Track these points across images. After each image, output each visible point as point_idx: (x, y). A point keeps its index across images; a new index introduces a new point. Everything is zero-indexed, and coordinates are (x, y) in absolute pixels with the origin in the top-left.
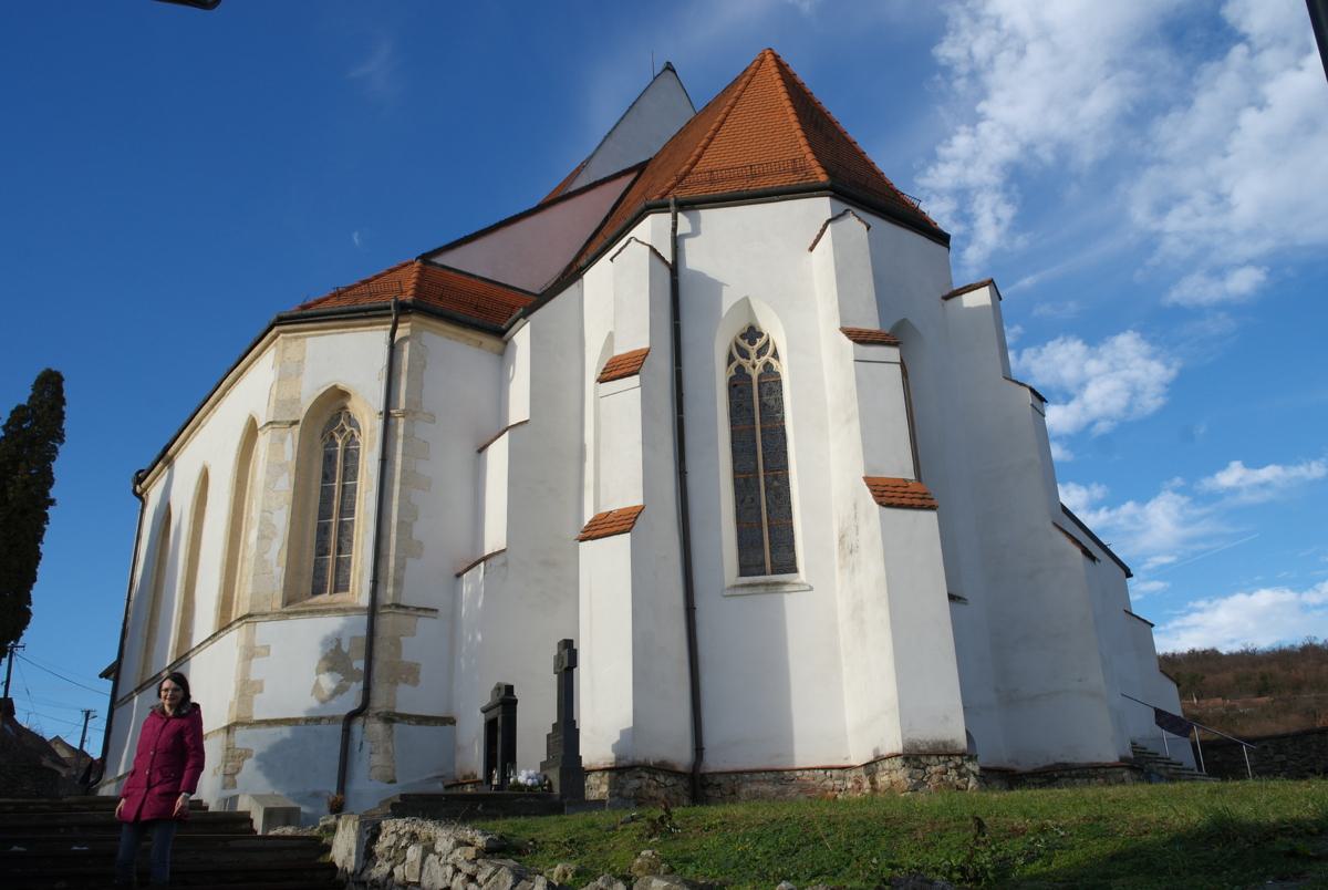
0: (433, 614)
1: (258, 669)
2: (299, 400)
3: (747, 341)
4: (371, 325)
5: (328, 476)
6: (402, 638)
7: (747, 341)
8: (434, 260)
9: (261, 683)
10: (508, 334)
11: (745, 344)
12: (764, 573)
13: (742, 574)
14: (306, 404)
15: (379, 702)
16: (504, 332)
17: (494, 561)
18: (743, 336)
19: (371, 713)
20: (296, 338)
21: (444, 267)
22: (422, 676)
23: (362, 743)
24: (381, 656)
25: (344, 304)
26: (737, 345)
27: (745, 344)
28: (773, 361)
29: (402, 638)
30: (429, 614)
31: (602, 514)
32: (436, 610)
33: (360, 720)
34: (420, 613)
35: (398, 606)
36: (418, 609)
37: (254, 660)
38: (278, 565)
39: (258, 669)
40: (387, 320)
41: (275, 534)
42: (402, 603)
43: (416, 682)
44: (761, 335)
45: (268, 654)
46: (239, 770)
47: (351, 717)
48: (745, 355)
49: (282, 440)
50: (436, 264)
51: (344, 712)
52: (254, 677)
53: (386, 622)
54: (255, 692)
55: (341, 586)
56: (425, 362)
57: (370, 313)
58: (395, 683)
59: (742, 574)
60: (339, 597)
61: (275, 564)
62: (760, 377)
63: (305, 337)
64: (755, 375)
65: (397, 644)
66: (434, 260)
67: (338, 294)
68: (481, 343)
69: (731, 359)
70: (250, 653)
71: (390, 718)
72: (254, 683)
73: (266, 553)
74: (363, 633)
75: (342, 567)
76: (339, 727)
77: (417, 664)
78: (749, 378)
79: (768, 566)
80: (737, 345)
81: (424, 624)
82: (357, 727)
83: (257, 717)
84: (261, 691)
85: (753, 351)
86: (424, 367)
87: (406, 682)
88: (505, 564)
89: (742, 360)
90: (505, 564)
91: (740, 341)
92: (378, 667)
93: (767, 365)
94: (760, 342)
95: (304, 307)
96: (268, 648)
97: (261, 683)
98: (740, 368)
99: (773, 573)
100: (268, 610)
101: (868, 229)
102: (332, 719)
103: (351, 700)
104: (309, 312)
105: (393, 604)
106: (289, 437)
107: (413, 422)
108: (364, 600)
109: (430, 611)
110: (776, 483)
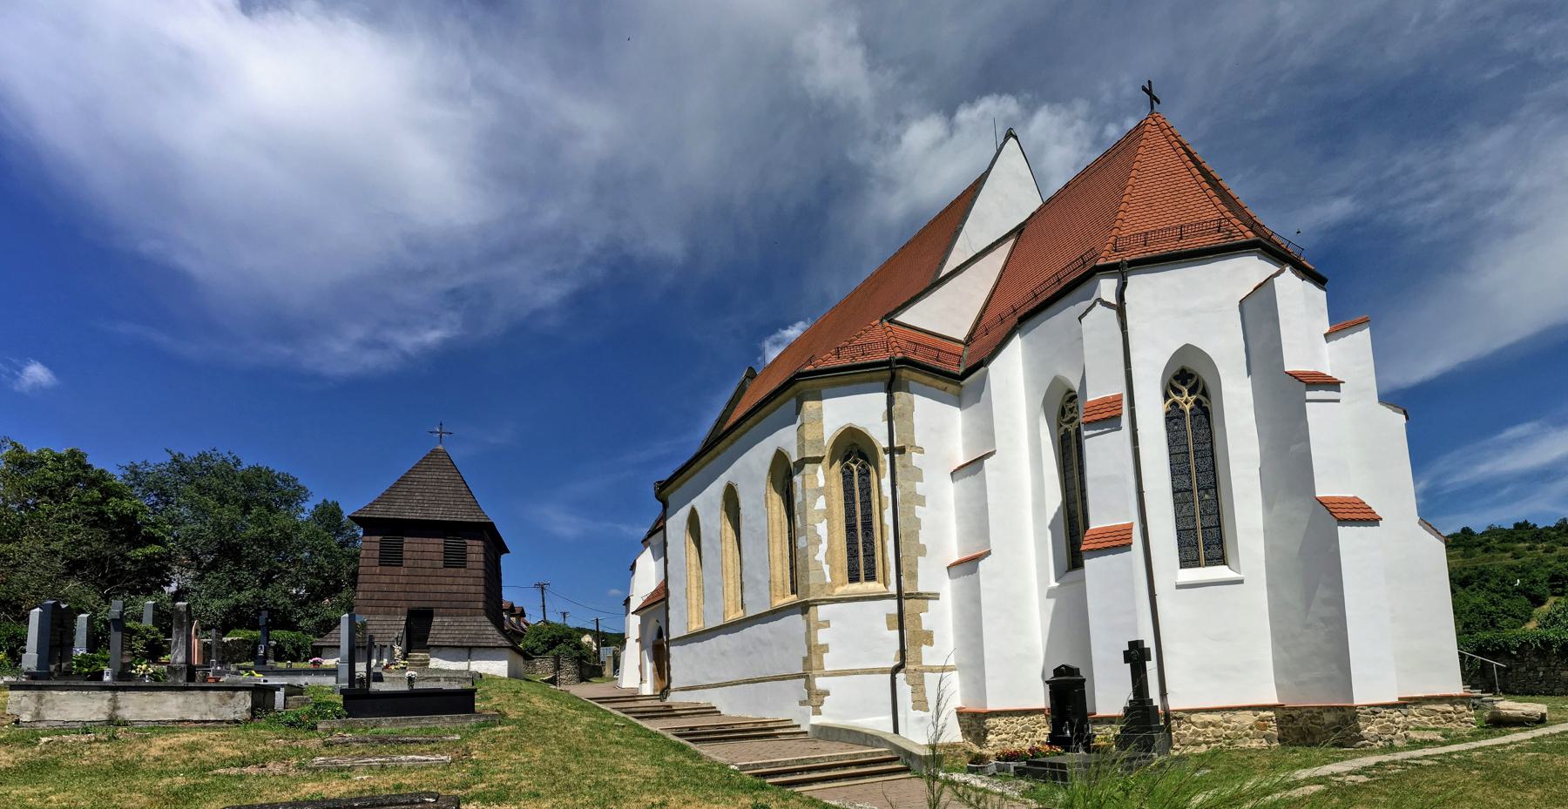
18: (1176, 378)
28: (1203, 398)
37: (819, 631)
39: (822, 636)
44: (1191, 376)
49: (816, 471)
53: (907, 604)
54: (824, 652)
59: (1186, 563)
61: (824, 562)
62: (1191, 410)
69: (1166, 397)
72: (823, 645)
74: (895, 611)
78: (1182, 411)
82: (900, 676)
94: (1191, 383)
96: (828, 622)
98: (1175, 404)
102: (883, 671)
103: (892, 662)
108: (893, 589)
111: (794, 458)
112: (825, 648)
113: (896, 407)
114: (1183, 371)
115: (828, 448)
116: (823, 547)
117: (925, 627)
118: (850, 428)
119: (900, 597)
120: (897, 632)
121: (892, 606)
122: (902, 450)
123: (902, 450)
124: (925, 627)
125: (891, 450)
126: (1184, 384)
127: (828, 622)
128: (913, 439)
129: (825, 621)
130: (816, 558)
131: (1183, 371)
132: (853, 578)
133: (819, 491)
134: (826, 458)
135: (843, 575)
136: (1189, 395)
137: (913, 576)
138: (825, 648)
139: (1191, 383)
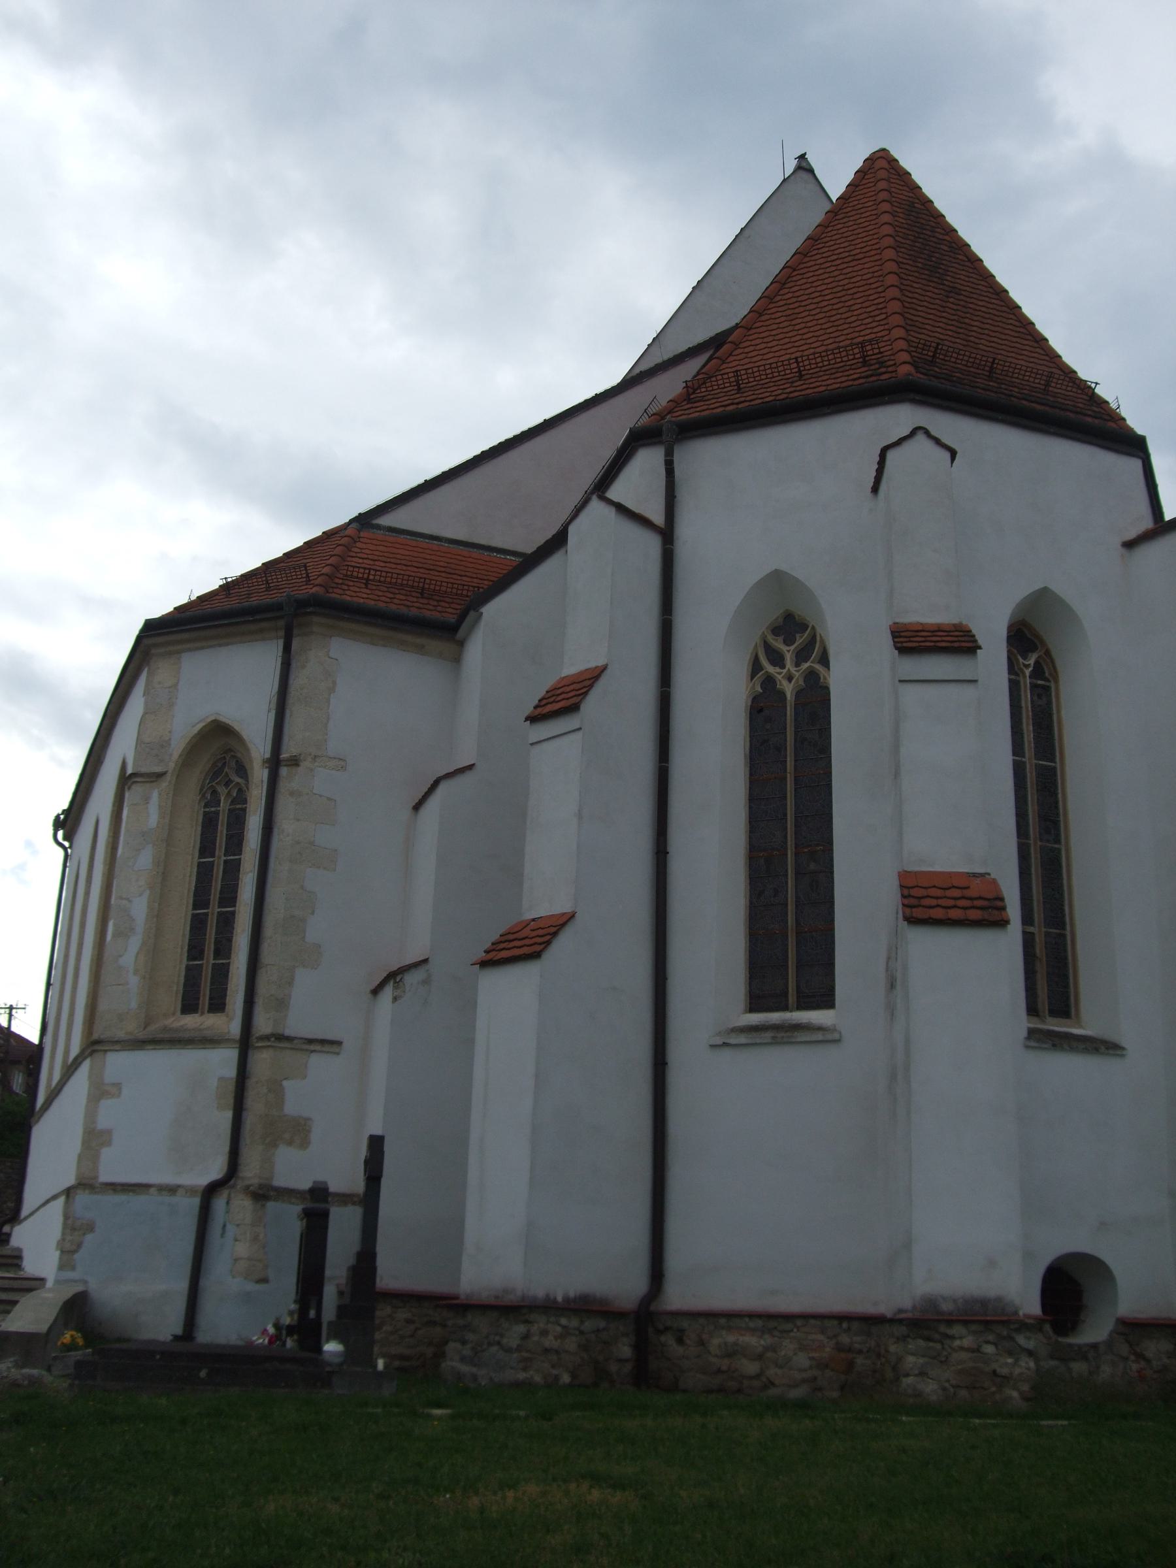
0: (335, 1048)
1: (108, 1114)
2: (168, 742)
3: (781, 639)
5: (206, 847)
6: (285, 1083)
7: (781, 639)
8: (376, 522)
9: (109, 1132)
10: (461, 634)
11: (778, 644)
12: (785, 1008)
13: (756, 1003)
14: (178, 746)
15: (251, 1172)
17: (411, 979)
18: (776, 631)
19: (240, 1184)
21: (391, 530)
22: (315, 1135)
23: (224, 1226)
24: (255, 1105)
26: (768, 648)
27: (778, 644)
28: (818, 667)
29: (285, 1083)
30: (327, 1048)
31: (522, 922)
32: (339, 1043)
33: (225, 1193)
34: (312, 1047)
35: (280, 1037)
36: (310, 1041)
38: (136, 972)
39: (108, 1114)
42: (287, 1032)
43: (305, 1144)
44: (803, 626)
45: (119, 1096)
46: (79, 1246)
47: (212, 1190)
48: (777, 659)
49: (147, 800)
50: (379, 527)
51: (204, 1181)
52: (103, 1123)
53: (262, 1061)
55: (218, 1005)
56: (334, 683)
57: (258, 617)
58: (274, 1145)
59: (752, 1009)
62: (799, 694)
63: (179, 652)
64: (789, 689)
65: (276, 1089)
66: (376, 522)
69: (756, 667)
70: (100, 1092)
71: (263, 1194)
73: (121, 956)
74: (231, 1072)
75: (222, 974)
76: (196, 1201)
77: (309, 1119)
78: (782, 695)
79: (792, 999)
80: (768, 648)
81: (318, 1062)
82: (219, 1204)
83: (104, 1177)
85: (789, 653)
86: (332, 689)
87: (290, 1143)
88: (426, 982)
89: (771, 669)
90: (426, 982)
91: (771, 639)
92: (249, 1120)
93: (812, 676)
94: (800, 640)
96: (118, 1086)
97: (109, 1132)
98: (769, 681)
99: (799, 1007)
100: (121, 1035)
101: (953, 458)
102: (191, 1191)
103: (215, 1170)
105: (273, 1035)
106: (155, 795)
107: (312, 770)
108: (235, 1028)
109: (330, 1045)
110: (812, 866)
113: (298, 680)
114: (789, 617)
115: (176, 755)
117: (291, 1107)
118: (215, 721)
119: (246, 1043)
120: (229, 1114)
121: (224, 1061)
122: (295, 762)
123: (295, 762)
124: (291, 1107)
125: (275, 763)
126: (788, 642)
127: (118, 1086)
129: (113, 1084)
131: (789, 617)
132: (189, 1006)
134: (169, 775)
135: (170, 998)
136: (797, 665)
137: (282, 1004)
139: (800, 640)
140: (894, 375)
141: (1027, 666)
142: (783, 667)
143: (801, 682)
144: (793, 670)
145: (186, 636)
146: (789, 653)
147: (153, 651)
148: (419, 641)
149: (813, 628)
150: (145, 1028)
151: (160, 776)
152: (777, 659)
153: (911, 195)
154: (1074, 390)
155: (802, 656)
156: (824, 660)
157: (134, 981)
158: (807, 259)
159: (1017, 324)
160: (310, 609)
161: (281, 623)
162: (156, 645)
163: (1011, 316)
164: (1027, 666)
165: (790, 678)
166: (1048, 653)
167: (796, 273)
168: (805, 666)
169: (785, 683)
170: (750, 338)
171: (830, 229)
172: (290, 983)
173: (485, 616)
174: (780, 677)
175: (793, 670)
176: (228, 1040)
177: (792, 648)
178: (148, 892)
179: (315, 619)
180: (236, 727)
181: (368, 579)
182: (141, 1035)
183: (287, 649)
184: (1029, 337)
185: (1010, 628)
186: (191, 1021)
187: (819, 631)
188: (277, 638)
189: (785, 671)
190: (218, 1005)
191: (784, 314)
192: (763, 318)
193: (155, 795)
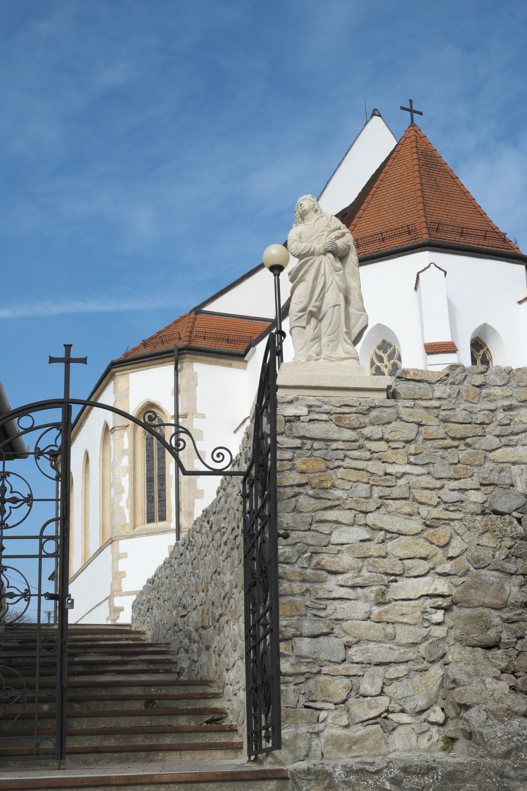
1: (122, 565)
3: (381, 351)
4: (164, 362)
7: (381, 351)
9: (124, 572)
11: (381, 353)
16: (244, 355)
18: (379, 348)
20: (123, 374)
25: (148, 351)
27: (381, 353)
37: (119, 561)
39: (122, 565)
40: (171, 359)
41: (123, 491)
44: (390, 345)
45: (127, 557)
48: (381, 359)
49: (122, 437)
52: (120, 570)
54: (122, 577)
55: (163, 518)
57: (162, 356)
60: (162, 524)
61: (125, 507)
63: (128, 373)
67: (145, 344)
68: (231, 364)
69: (372, 363)
72: (122, 573)
84: (125, 577)
85: (385, 357)
91: (377, 351)
95: (126, 355)
96: (126, 554)
97: (124, 572)
100: (124, 533)
104: (129, 357)
106: (126, 434)
108: (173, 525)
111: (111, 427)
112: (123, 574)
114: (384, 341)
116: (126, 495)
123: (185, 416)
126: (385, 352)
127: (126, 554)
128: (195, 408)
129: (124, 553)
130: (121, 504)
131: (384, 341)
132: (150, 519)
133: (124, 452)
135: (141, 517)
136: (389, 361)
138: (123, 574)
140: (421, 239)
141: (479, 355)
142: (383, 362)
143: (391, 368)
144: (387, 363)
145: (133, 366)
146: (385, 357)
147: (116, 374)
148: (230, 362)
149: (394, 346)
150: (134, 528)
151: (127, 426)
152: (381, 359)
153: (426, 147)
154: (497, 236)
155: (390, 358)
156: (399, 359)
157: (127, 512)
158: (382, 183)
159: (474, 207)
160: (185, 352)
161: (173, 358)
162: (117, 372)
163: (471, 204)
164: (479, 355)
165: (386, 367)
166: (488, 349)
167: (378, 190)
168: (392, 361)
169: (384, 369)
170: (361, 222)
171: (392, 167)
172: (193, 505)
173: (257, 350)
174: (382, 367)
175: (387, 363)
176: (172, 530)
177: (386, 355)
178: (128, 475)
179: (187, 355)
180: (158, 404)
181: (205, 337)
182: (132, 532)
183: (176, 369)
184: (478, 213)
185: (471, 341)
186: (152, 525)
187: (396, 347)
188: (172, 364)
189: (384, 364)
190: (163, 518)
191: (374, 210)
192: (365, 213)
193: (126, 434)
